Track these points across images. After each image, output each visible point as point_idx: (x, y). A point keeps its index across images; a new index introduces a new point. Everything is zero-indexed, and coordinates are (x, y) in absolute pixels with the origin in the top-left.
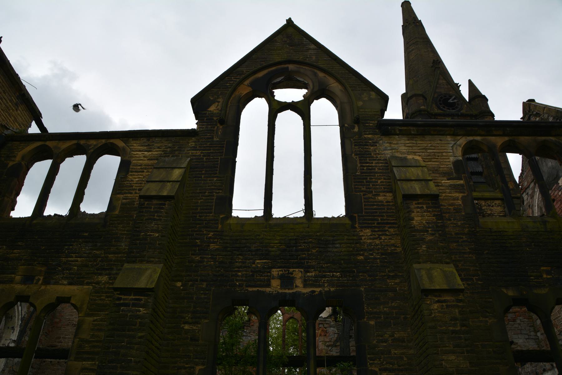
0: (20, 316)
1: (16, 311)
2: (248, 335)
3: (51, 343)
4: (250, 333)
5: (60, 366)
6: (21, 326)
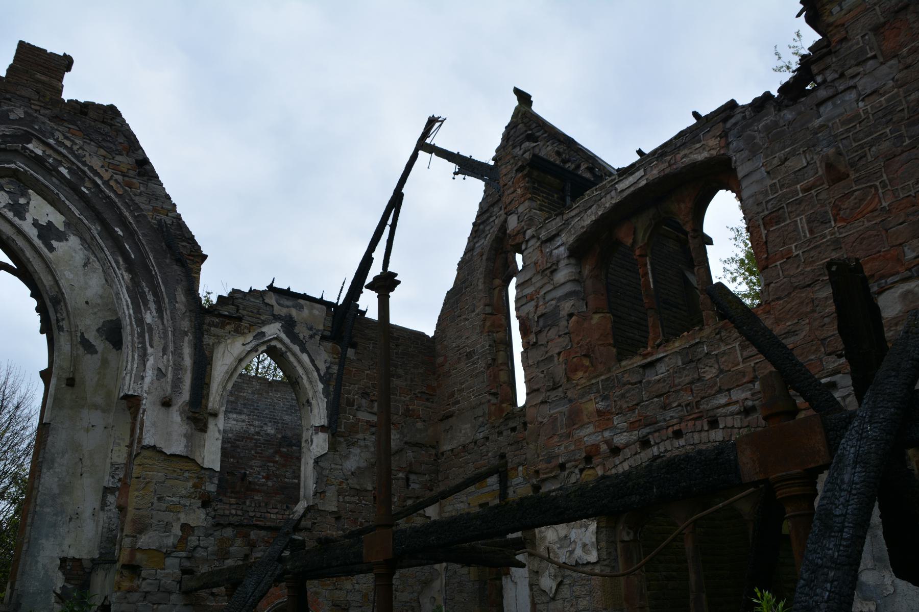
0: (315, 374)
1: (296, 364)
2: (842, 88)
3: (444, 411)
4: (842, 75)
5: (469, 454)
6: (326, 393)
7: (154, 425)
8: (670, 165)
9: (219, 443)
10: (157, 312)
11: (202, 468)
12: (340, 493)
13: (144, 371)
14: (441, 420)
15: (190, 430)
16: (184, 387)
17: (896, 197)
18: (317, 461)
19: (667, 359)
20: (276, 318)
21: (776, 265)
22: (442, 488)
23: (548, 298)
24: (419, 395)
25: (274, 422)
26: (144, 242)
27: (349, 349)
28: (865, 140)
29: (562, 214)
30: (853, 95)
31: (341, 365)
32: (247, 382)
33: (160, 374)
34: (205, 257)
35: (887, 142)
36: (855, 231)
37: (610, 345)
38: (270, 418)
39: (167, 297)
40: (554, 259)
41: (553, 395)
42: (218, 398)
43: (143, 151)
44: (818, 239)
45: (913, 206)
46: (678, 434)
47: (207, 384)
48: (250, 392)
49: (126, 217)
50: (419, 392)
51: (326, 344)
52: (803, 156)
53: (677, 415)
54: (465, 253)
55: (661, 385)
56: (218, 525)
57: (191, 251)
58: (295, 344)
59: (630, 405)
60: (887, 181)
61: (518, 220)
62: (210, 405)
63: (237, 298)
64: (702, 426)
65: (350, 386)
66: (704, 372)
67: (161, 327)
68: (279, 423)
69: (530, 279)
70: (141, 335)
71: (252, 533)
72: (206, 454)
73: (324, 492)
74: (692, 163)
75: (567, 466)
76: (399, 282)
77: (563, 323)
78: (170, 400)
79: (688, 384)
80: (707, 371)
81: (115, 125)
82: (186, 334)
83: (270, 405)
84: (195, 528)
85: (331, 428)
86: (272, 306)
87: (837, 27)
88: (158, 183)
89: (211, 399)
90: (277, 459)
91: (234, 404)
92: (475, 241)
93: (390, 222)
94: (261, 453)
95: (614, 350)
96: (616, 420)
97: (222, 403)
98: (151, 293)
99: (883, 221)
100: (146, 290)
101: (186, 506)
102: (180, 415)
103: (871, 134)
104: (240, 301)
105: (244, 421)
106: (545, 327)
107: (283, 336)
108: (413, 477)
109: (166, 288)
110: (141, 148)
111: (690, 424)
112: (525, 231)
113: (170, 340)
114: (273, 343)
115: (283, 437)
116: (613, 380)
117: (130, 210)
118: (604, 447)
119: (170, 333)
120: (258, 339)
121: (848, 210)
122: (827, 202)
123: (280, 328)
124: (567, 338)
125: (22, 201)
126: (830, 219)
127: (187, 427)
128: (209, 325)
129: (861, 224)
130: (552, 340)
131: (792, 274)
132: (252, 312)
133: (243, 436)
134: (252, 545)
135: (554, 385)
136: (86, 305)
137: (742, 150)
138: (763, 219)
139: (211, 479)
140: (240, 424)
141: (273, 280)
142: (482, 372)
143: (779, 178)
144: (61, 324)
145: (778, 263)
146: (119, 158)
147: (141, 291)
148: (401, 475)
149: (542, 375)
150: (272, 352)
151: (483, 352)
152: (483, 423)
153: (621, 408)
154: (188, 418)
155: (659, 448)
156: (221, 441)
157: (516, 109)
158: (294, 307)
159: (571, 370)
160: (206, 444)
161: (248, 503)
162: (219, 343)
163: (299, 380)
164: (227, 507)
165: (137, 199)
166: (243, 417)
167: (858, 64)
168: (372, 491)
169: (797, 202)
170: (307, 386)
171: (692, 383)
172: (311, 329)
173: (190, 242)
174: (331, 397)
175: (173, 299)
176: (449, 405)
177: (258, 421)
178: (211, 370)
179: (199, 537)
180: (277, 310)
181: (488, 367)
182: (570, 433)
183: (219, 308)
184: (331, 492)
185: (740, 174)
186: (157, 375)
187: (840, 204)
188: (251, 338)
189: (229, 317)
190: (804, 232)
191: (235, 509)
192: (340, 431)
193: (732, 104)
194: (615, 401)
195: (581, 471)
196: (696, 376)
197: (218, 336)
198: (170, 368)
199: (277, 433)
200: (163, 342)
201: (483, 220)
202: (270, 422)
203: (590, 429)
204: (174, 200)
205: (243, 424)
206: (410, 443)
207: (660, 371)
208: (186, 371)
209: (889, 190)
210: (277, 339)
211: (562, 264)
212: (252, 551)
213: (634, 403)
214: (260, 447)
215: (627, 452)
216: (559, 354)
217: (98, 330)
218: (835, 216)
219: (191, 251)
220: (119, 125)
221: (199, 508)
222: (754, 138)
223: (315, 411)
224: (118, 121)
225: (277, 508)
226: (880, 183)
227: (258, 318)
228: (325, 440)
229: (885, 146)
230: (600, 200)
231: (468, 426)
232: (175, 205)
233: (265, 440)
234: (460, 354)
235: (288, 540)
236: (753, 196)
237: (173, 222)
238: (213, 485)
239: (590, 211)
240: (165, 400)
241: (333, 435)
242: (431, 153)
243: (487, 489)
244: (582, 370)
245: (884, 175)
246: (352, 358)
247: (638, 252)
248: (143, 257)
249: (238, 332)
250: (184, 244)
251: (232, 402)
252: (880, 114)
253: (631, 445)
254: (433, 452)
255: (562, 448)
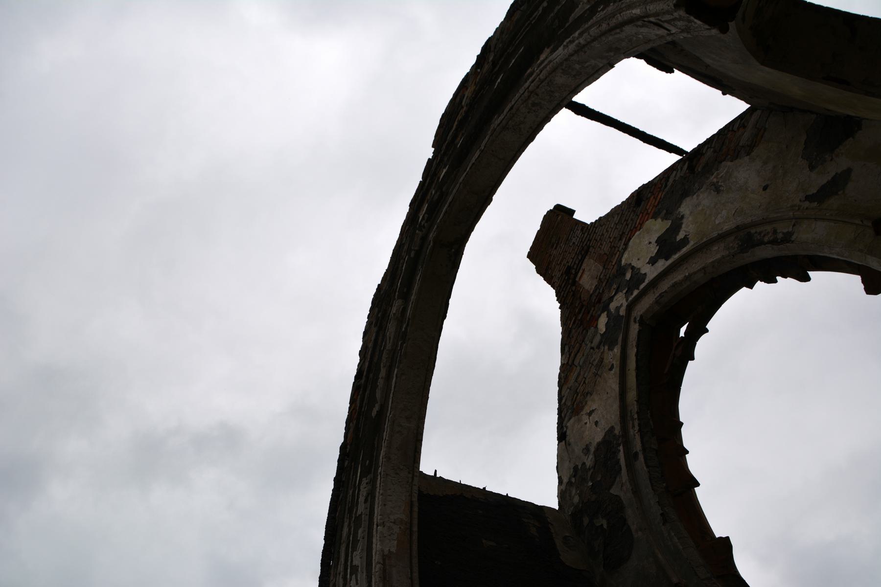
125: (628, 276)
136: (768, 191)
144: (780, 236)
217: (812, 168)
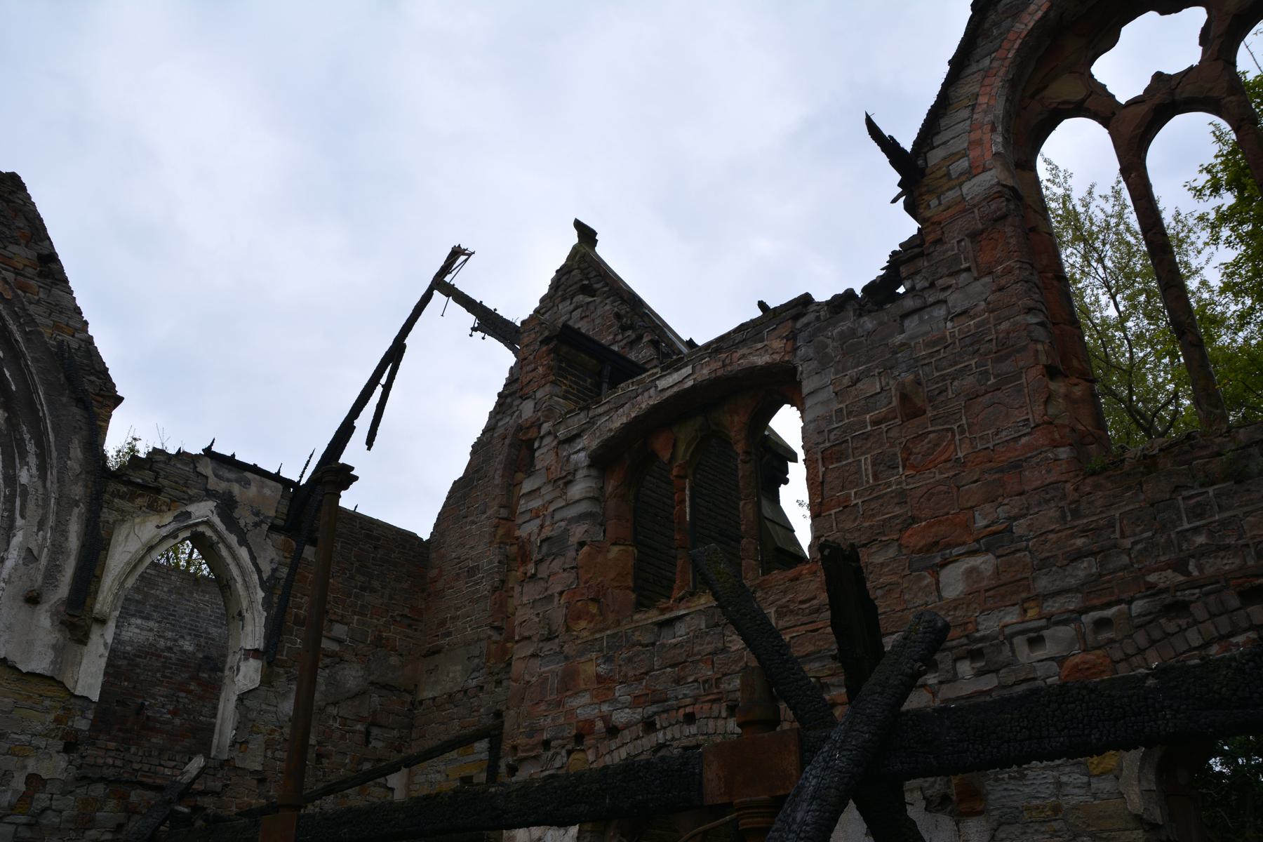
0: (256, 577)
1: (229, 560)
2: (931, 300)
3: (429, 643)
4: (932, 285)
5: (456, 706)
6: (267, 604)
7: (8, 628)
8: (724, 366)
9: (103, 661)
10: (38, 470)
11: (73, 695)
12: (269, 745)
13: (6, 550)
14: (425, 656)
15: (61, 640)
16: (63, 579)
17: (973, 448)
18: (241, 698)
19: (688, 619)
20: (210, 494)
21: (831, 514)
22: (414, 749)
23: (558, 516)
24: (398, 619)
25: (195, 635)
26: (33, 370)
27: (307, 547)
28: (948, 371)
29: (587, 408)
30: (941, 312)
31: (293, 568)
32: (165, 576)
33: (30, 556)
34: (120, 399)
35: (971, 377)
36: (924, 483)
37: (628, 588)
38: (189, 629)
39: (56, 450)
40: (571, 467)
41: (547, 647)
42: (110, 599)
43: (51, 243)
44: (882, 487)
45: (991, 461)
46: (690, 719)
47: (97, 577)
48: (165, 589)
49: (12, 331)
50: (398, 615)
51: (275, 536)
52: (877, 379)
53: (691, 694)
54: (484, 432)
55: (678, 651)
56: (84, 779)
57: (101, 390)
58: (231, 532)
59: (637, 673)
60: (966, 426)
61: (535, 407)
62: (98, 607)
63: (156, 462)
64: (720, 713)
65: (302, 598)
66: (730, 642)
67: (41, 491)
68: (202, 636)
69: (539, 489)
70: (10, 500)
71: (133, 793)
72: (82, 675)
73: (246, 742)
74: (750, 367)
75: (553, 744)
76: (356, 478)
77: (572, 553)
78: (39, 595)
79: (710, 654)
80: (734, 640)
81: (14, 202)
82: (76, 504)
83: (192, 611)
84: (48, 782)
85: (268, 655)
86: (207, 477)
87: (933, 224)
88: (67, 290)
89: (100, 598)
90: (192, 688)
91: (130, 607)
92: (498, 417)
93: (383, 380)
94: (171, 678)
95: (633, 596)
96: (619, 690)
97: (115, 605)
98: (33, 442)
99: (955, 475)
100: (27, 437)
101: (39, 748)
102: (51, 617)
103: (956, 363)
104: (162, 465)
105: (151, 630)
106: (548, 555)
107: (216, 520)
108: (375, 731)
109: (56, 437)
110: (49, 239)
111: (706, 706)
112: (542, 424)
113: (51, 511)
114: (201, 529)
115: (206, 658)
116: (621, 637)
117: (20, 322)
118: (599, 725)
119: (53, 500)
120: (179, 521)
121: (920, 455)
122: (898, 441)
123: (213, 509)
124: (573, 575)
126: (898, 464)
127: (58, 635)
128: (113, 495)
129: (932, 475)
130: (555, 574)
131: (846, 528)
132: (176, 482)
133: (147, 652)
134: (131, 811)
135: (549, 634)
137: (811, 360)
138: (822, 452)
139: (83, 712)
140: (145, 633)
141: (213, 442)
142: (486, 597)
143: (848, 403)
145: (833, 512)
146: (13, 248)
147: (18, 437)
148: (359, 727)
149: (537, 620)
150: (198, 540)
151: (490, 569)
152: (478, 665)
153: (626, 675)
154: (62, 623)
155: (665, 734)
156: (106, 659)
157: (574, 248)
158: (237, 481)
159: (574, 616)
160: (84, 661)
161: (133, 750)
162: (123, 521)
163: (232, 583)
164: (102, 753)
165: (32, 309)
166: (151, 624)
167: (951, 275)
168: (314, 746)
169: (864, 436)
170: (241, 594)
171: (714, 653)
172: (257, 514)
173: (102, 376)
174: (274, 611)
175: (64, 452)
176: (437, 636)
177: (172, 632)
178: (106, 558)
179: (52, 794)
180: (213, 483)
181: (494, 591)
182: (560, 701)
183: (130, 472)
184: (257, 744)
185: (805, 391)
186: (24, 559)
187: (911, 446)
188: (171, 519)
189: (144, 487)
190: (867, 475)
191: (113, 757)
192: (279, 659)
193: (806, 299)
194: (620, 666)
195: (569, 753)
196: (720, 645)
197: (123, 511)
198: (46, 549)
199: (198, 650)
200: (41, 511)
201: (512, 391)
202: (190, 634)
203: (586, 698)
204: (86, 316)
205: (151, 634)
206: (377, 683)
207: (679, 634)
208: (68, 557)
209: (966, 437)
210: (208, 523)
211: (581, 474)
212: (129, 819)
213: (643, 671)
214: (171, 668)
215: (627, 735)
216: (561, 593)
218: (905, 460)
219: (101, 390)
220: (22, 203)
221: (58, 752)
222: (827, 346)
223: (249, 628)
224: (20, 196)
225: (175, 760)
226: (958, 427)
227: (184, 492)
228: (256, 671)
229: (969, 381)
230: (636, 398)
231: (459, 668)
232: (86, 323)
233: (178, 660)
234: (460, 569)
235: (168, 812)
236: (815, 420)
237: (80, 346)
238: (84, 721)
239: (621, 410)
240: (30, 594)
241: (269, 664)
242: (448, 296)
243: (472, 758)
244: (585, 619)
245: (964, 418)
246: (310, 559)
247: (675, 472)
248: (28, 391)
249: (154, 508)
250: (93, 378)
251: (138, 602)
252: (968, 341)
253: (631, 726)
254: (408, 698)
255: (549, 720)
